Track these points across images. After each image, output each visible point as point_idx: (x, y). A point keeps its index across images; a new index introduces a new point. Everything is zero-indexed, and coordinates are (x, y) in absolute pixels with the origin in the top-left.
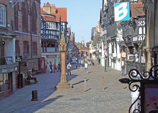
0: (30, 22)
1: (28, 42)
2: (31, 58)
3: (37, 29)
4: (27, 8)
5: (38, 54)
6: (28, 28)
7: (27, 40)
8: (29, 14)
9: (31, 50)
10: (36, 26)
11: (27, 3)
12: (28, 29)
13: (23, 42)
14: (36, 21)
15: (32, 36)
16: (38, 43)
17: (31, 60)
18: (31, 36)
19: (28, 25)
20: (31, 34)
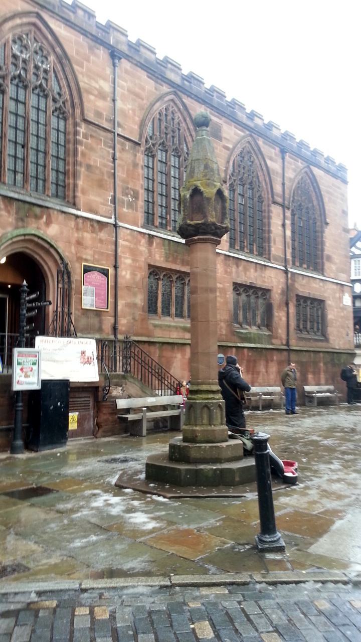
0: (280, 228)
1: (266, 292)
2: (285, 347)
3: (329, 258)
4: (267, 179)
5: (331, 338)
6: (269, 247)
7: (266, 285)
8: (275, 203)
9: (284, 319)
10: (322, 250)
11: (263, 163)
12: (269, 251)
13: (232, 284)
14: (322, 232)
15: (289, 275)
16: (329, 302)
17: (285, 353)
18: (286, 272)
19: (269, 238)
20: (285, 267)
